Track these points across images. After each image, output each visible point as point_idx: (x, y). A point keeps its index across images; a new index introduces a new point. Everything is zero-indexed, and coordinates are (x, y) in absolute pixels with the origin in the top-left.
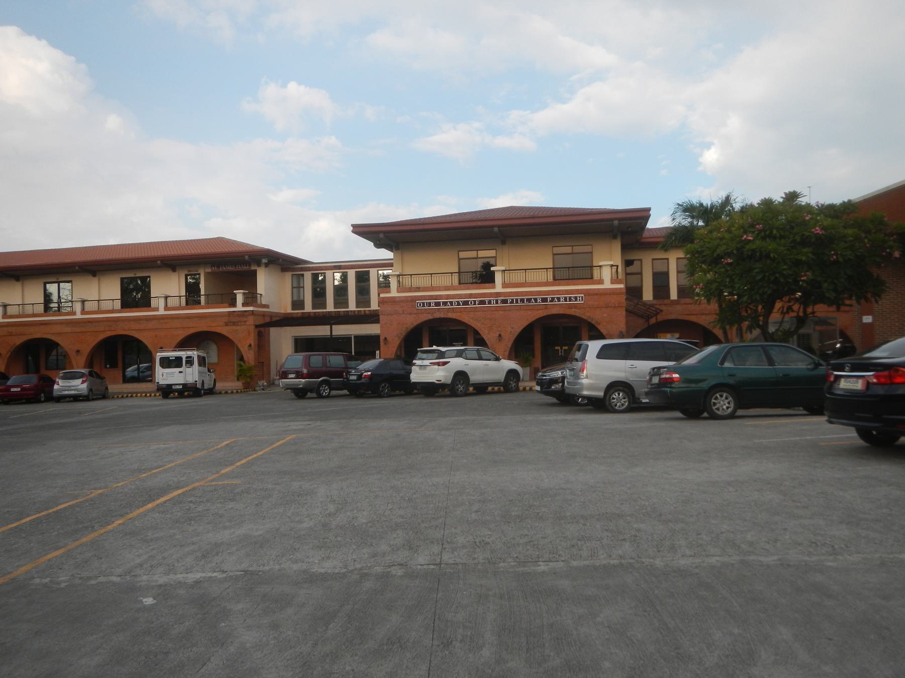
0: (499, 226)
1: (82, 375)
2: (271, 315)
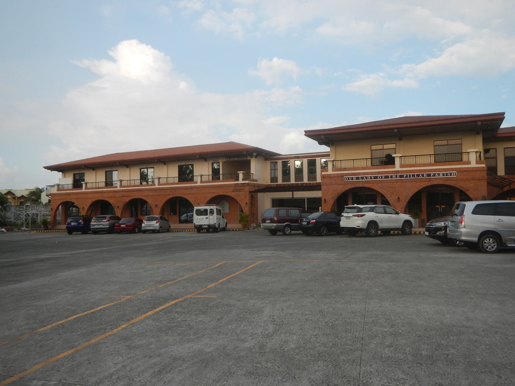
0: (397, 128)
1: (157, 219)
2: (259, 186)
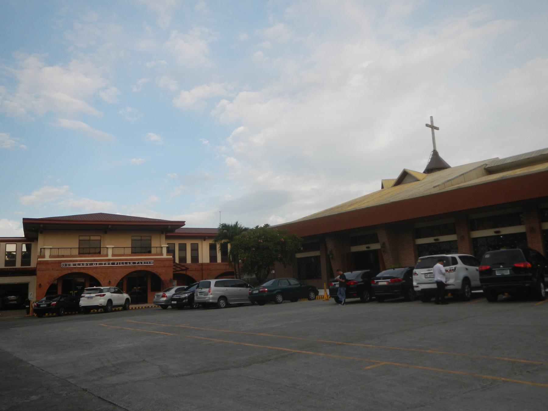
0: (112, 225)
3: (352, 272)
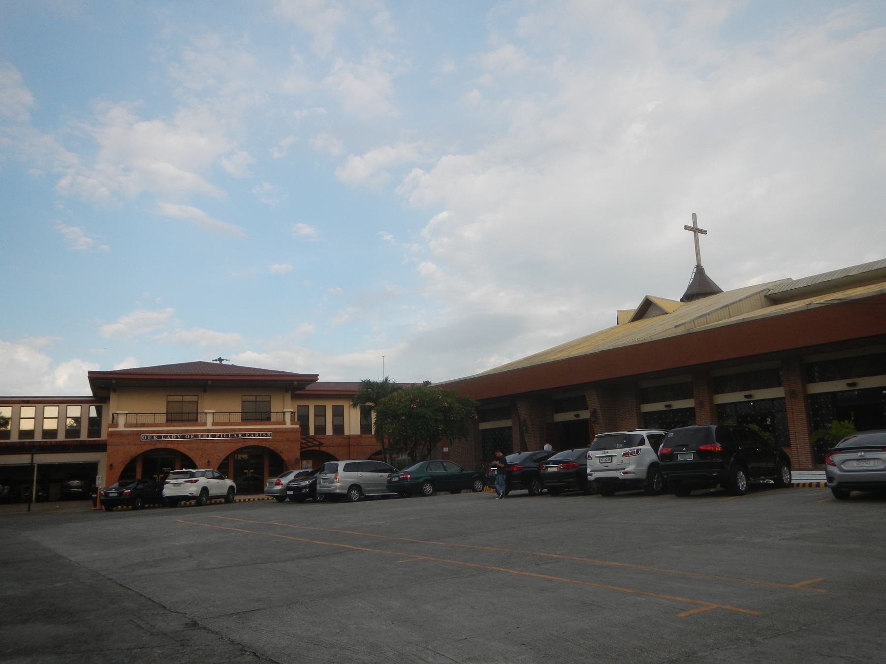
0: (212, 380)
3: (520, 454)
